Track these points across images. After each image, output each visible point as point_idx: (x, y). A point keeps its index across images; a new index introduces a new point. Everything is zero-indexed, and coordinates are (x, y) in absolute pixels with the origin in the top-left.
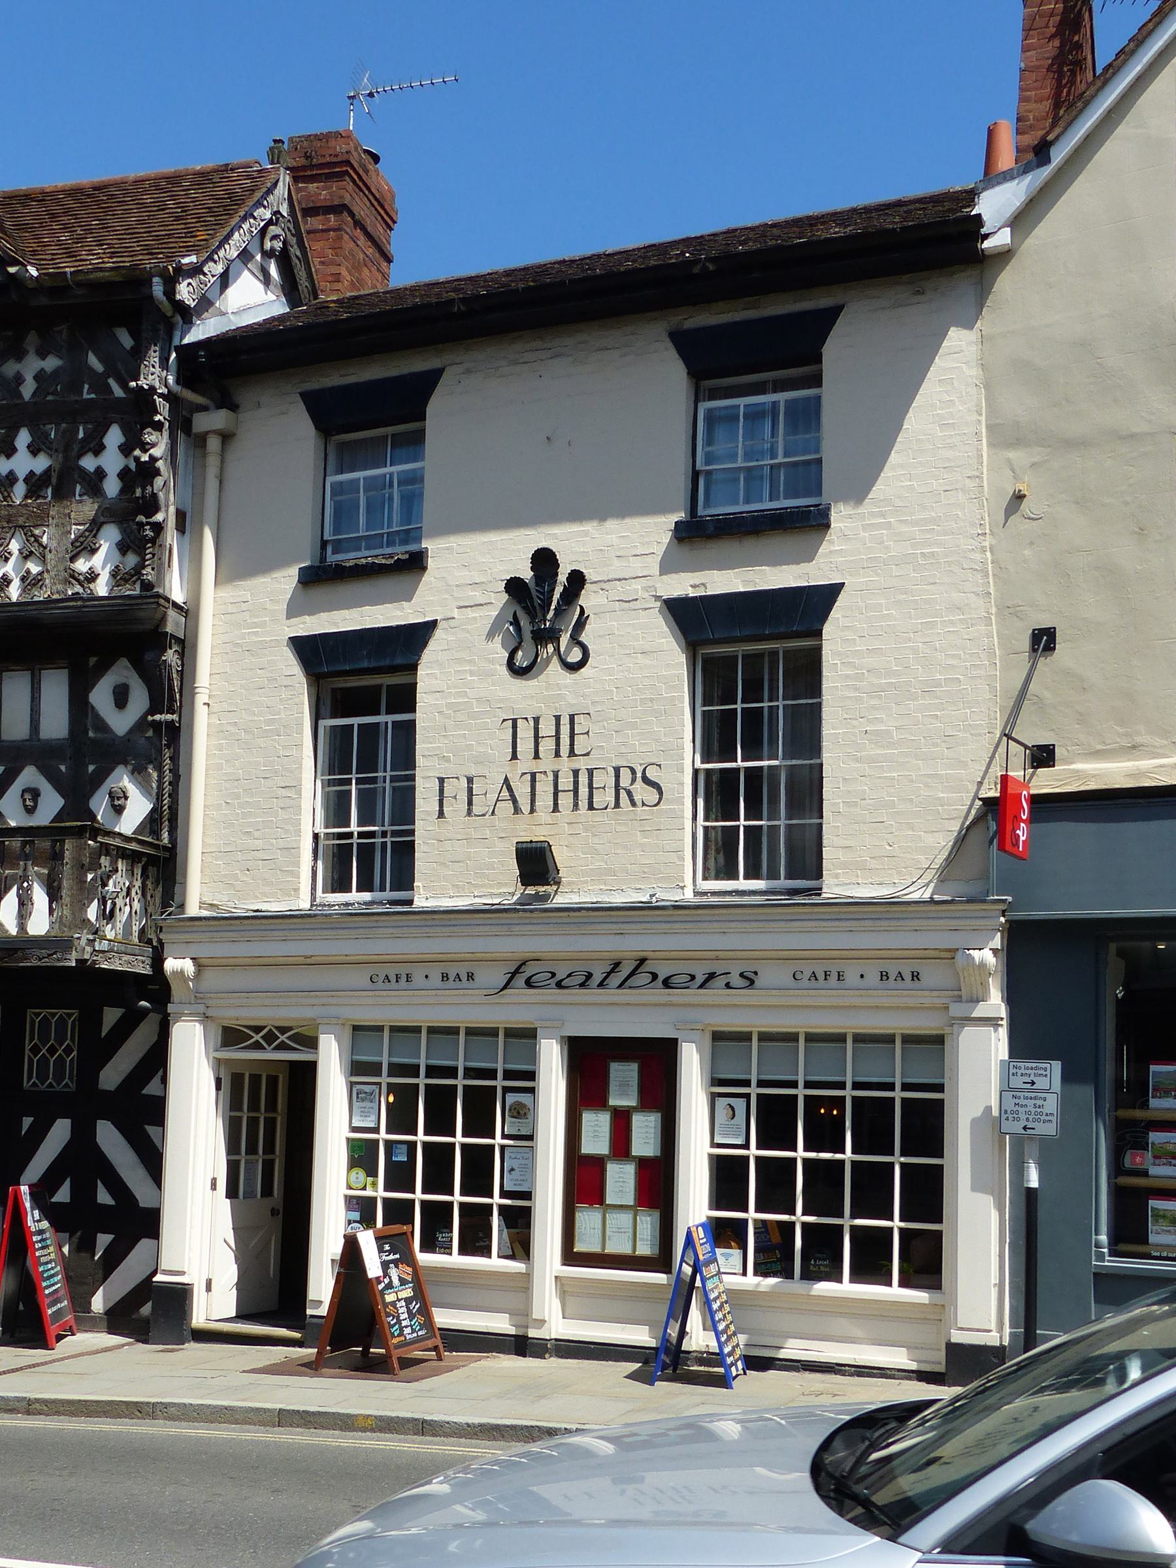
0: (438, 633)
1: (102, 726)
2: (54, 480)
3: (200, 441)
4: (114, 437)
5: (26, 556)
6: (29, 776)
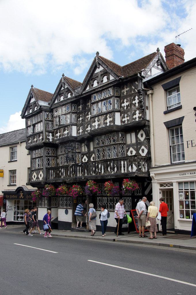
1: (140, 140)
3: (149, 95)
4: (137, 98)
5: (127, 117)
6: (131, 149)
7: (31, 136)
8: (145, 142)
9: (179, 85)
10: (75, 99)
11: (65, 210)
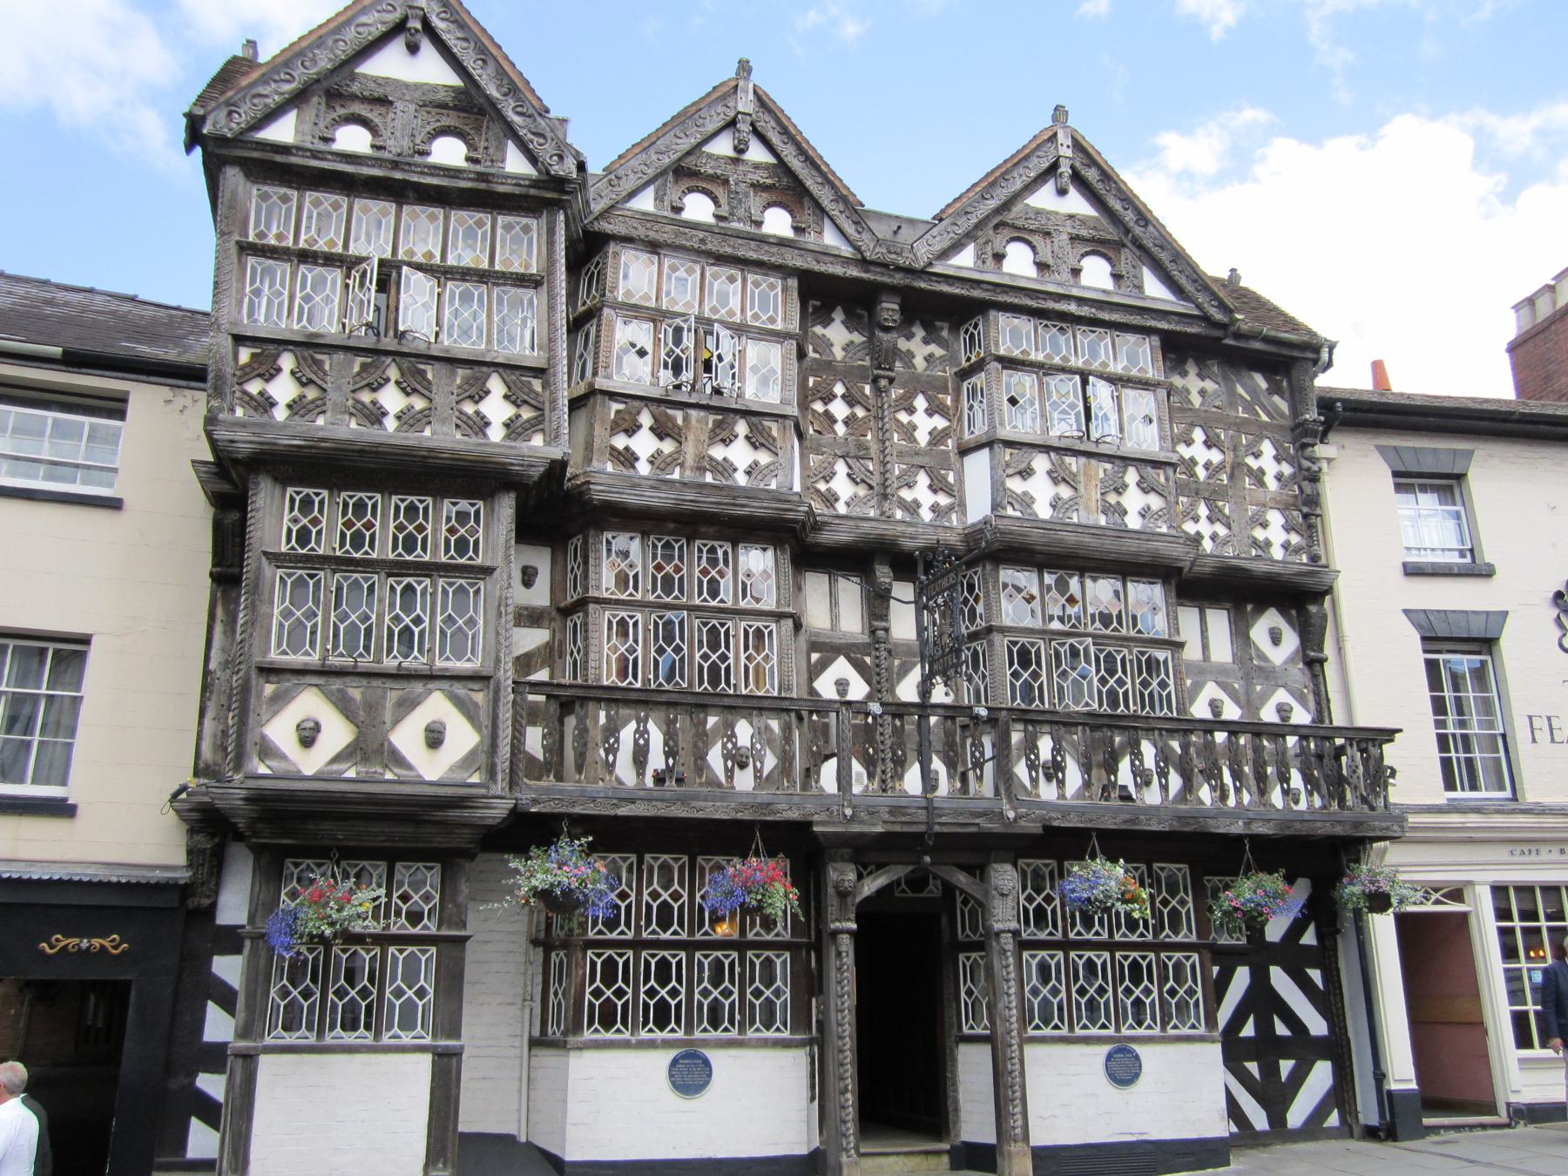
0: (1508, 620)
1: (1263, 657)
2: (1228, 469)
4: (1267, 448)
7: (310, 347)
8: (1298, 672)
9: (1460, 477)
10: (854, 272)
11: (664, 1058)
